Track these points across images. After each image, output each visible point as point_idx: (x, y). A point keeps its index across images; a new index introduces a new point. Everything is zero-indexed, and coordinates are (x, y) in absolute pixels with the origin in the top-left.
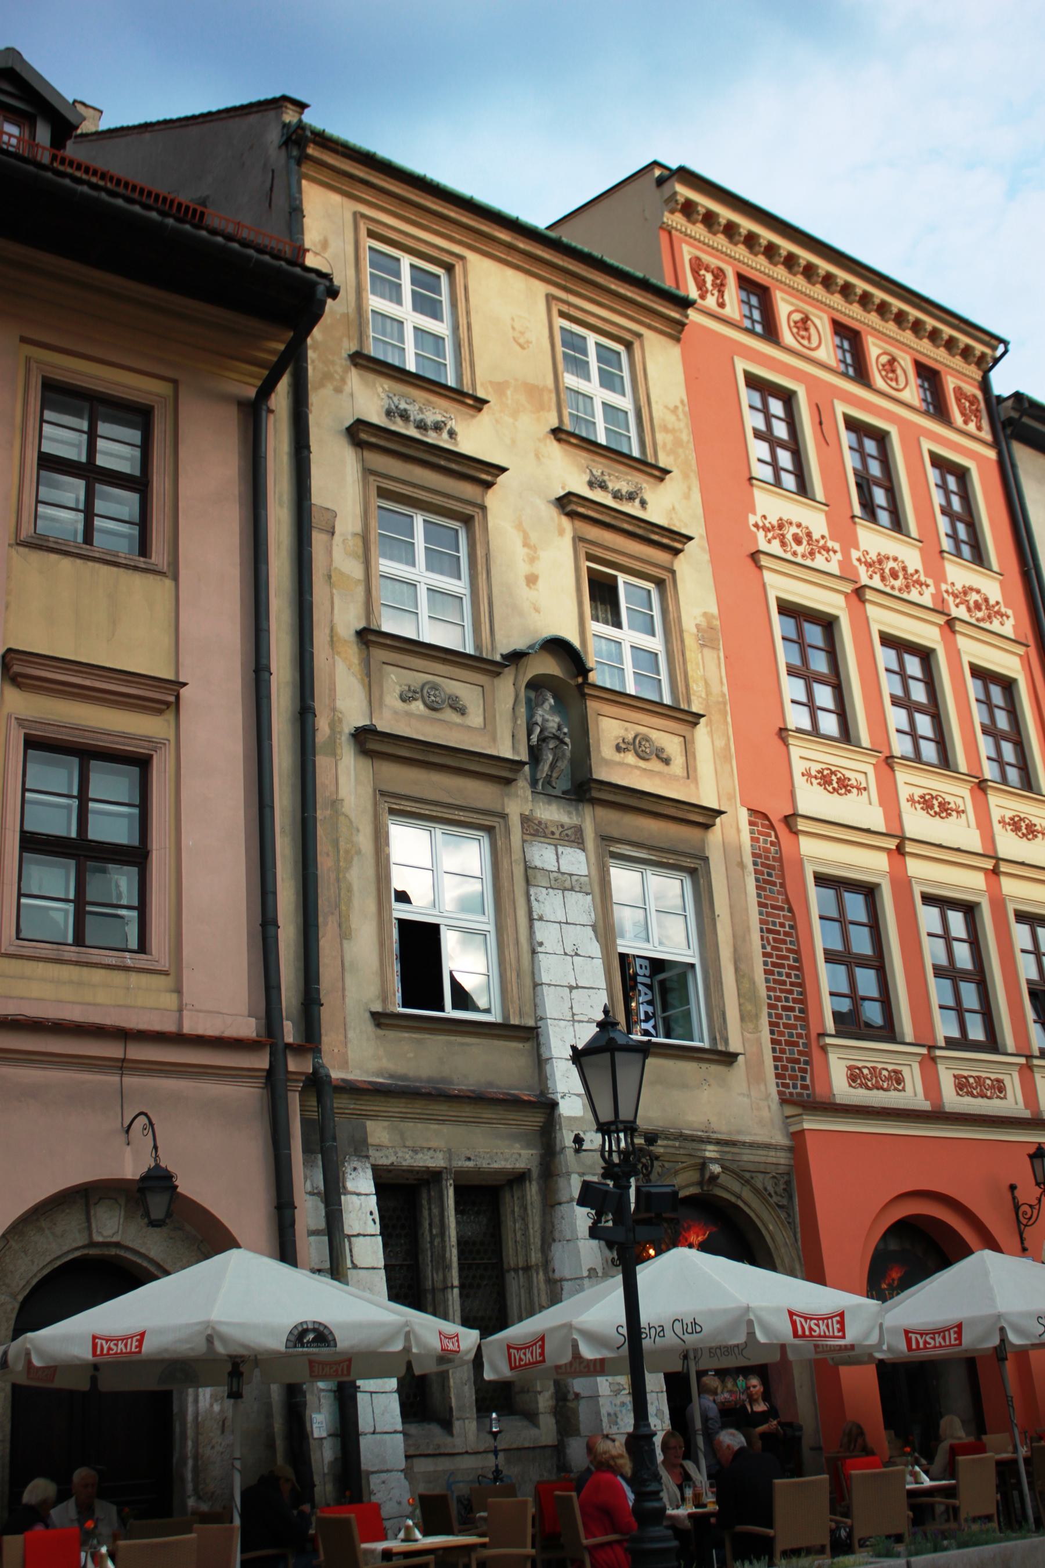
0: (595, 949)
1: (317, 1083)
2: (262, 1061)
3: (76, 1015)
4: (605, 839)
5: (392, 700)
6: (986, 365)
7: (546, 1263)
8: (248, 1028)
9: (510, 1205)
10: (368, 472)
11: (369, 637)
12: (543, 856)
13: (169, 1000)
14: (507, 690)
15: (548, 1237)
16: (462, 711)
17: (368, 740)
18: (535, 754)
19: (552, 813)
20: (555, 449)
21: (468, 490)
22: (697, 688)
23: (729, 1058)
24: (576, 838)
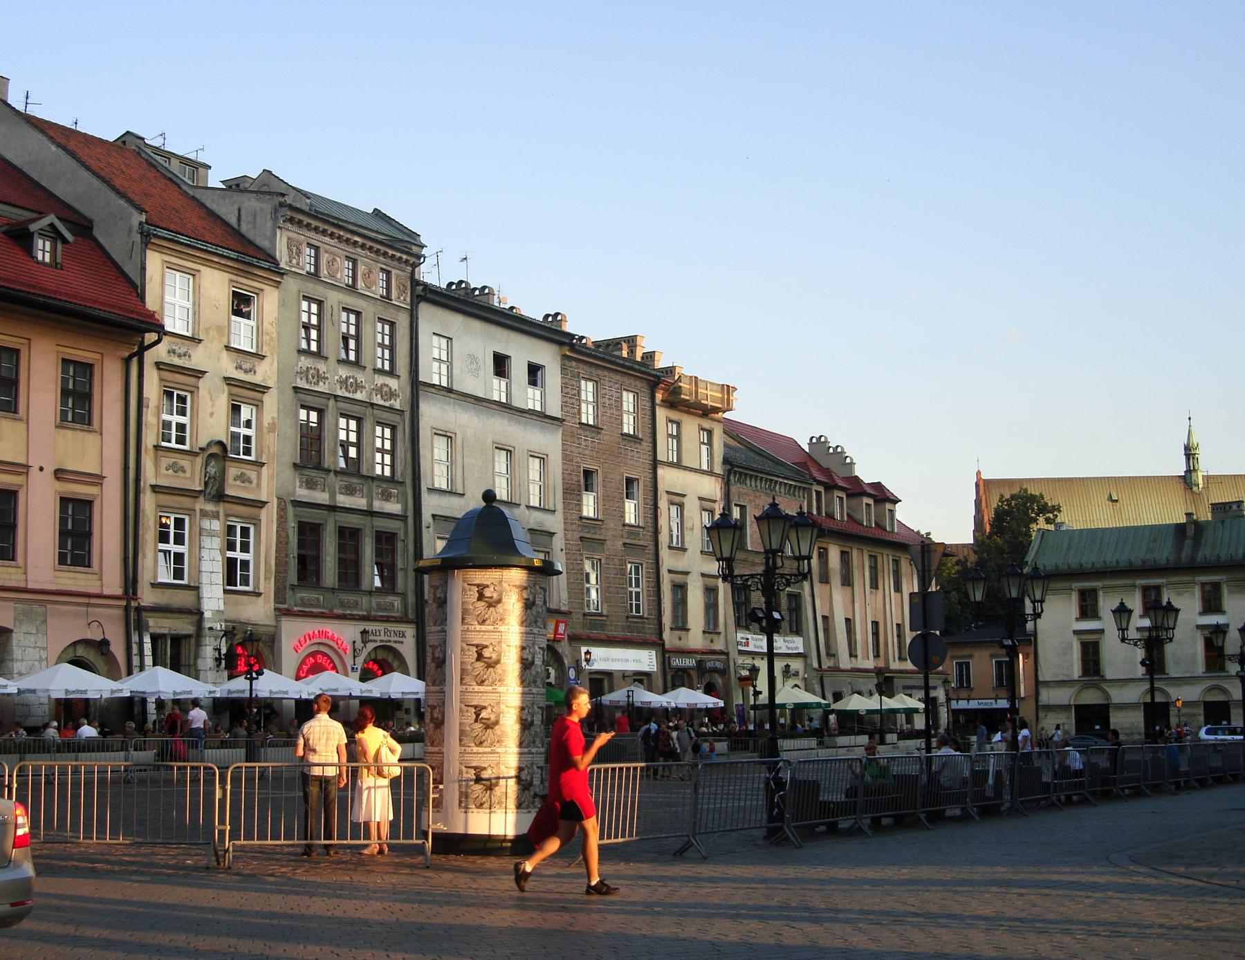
0: (220, 558)
1: (139, 609)
2: (124, 603)
3: (74, 589)
4: (227, 515)
5: (164, 471)
6: (415, 266)
7: (195, 664)
8: (120, 592)
9: (184, 643)
10: (161, 380)
11: (157, 447)
12: (206, 524)
13: (98, 583)
14: (199, 461)
15: (197, 656)
16: (184, 472)
17: (155, 489)
18: (206, 484)
19: (210, 507)
20: (225, 353)
21: (191, 380)
22: (265, 450)
23: (259, 595)
24: (216, 516)
